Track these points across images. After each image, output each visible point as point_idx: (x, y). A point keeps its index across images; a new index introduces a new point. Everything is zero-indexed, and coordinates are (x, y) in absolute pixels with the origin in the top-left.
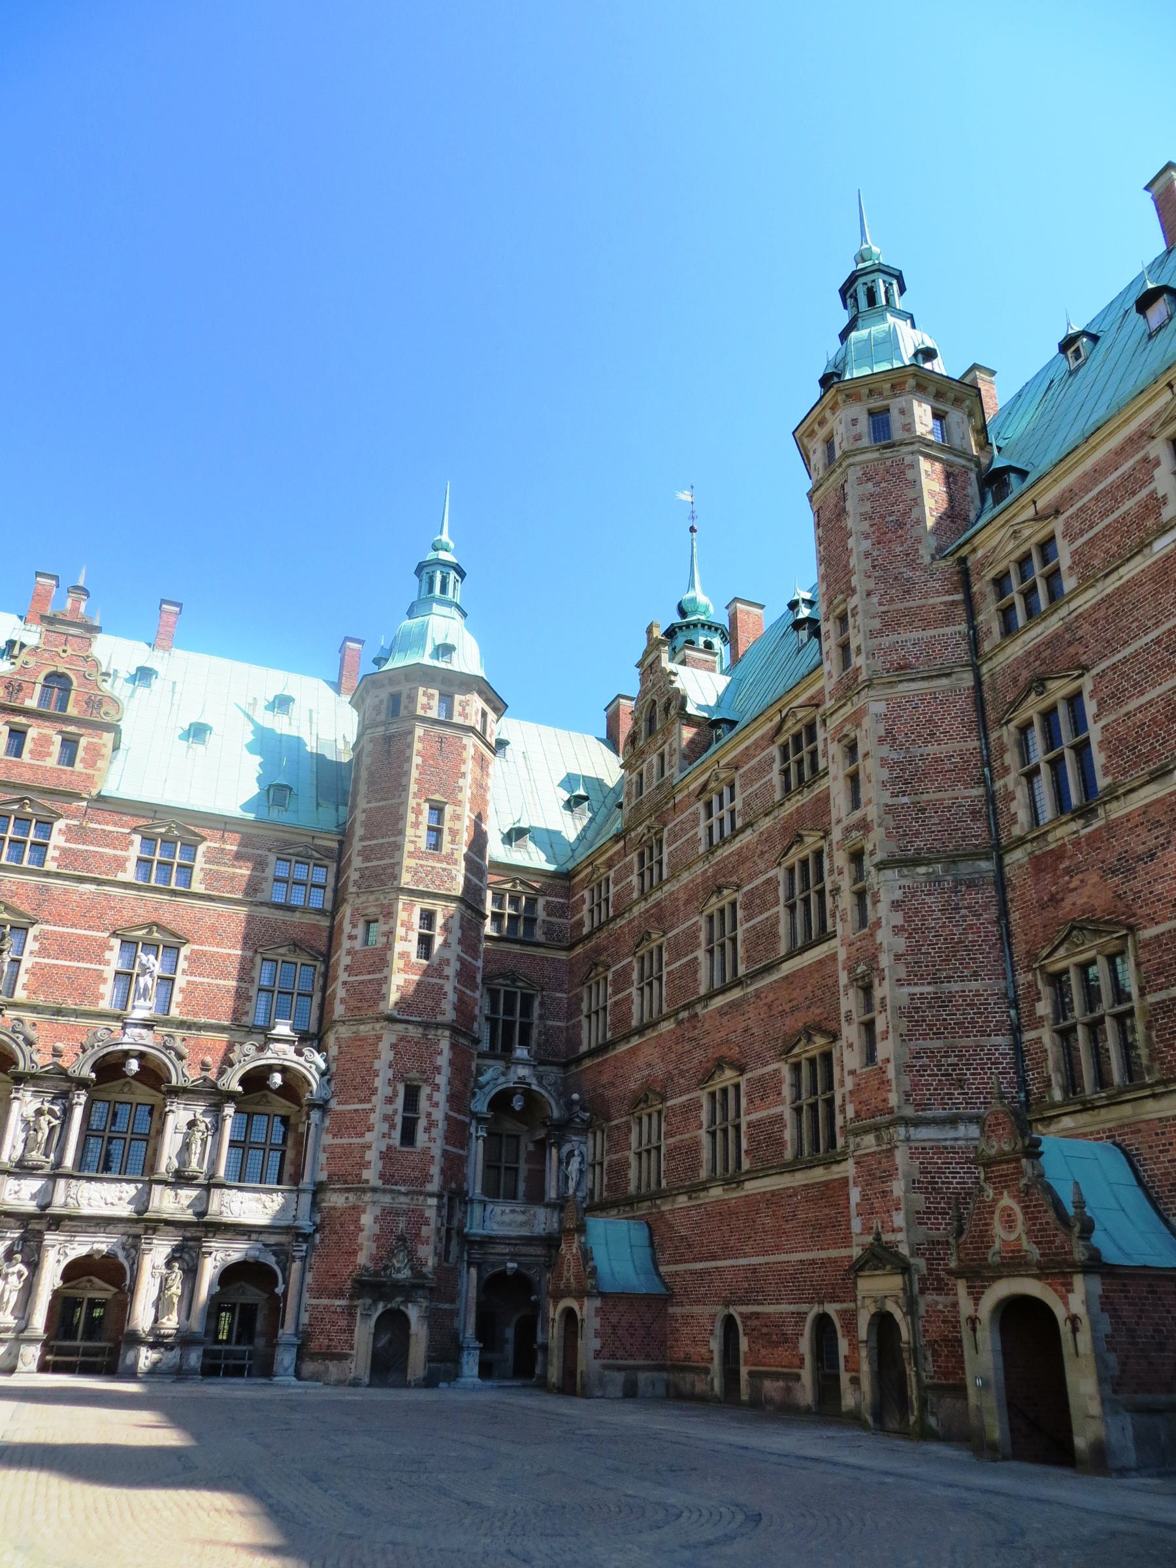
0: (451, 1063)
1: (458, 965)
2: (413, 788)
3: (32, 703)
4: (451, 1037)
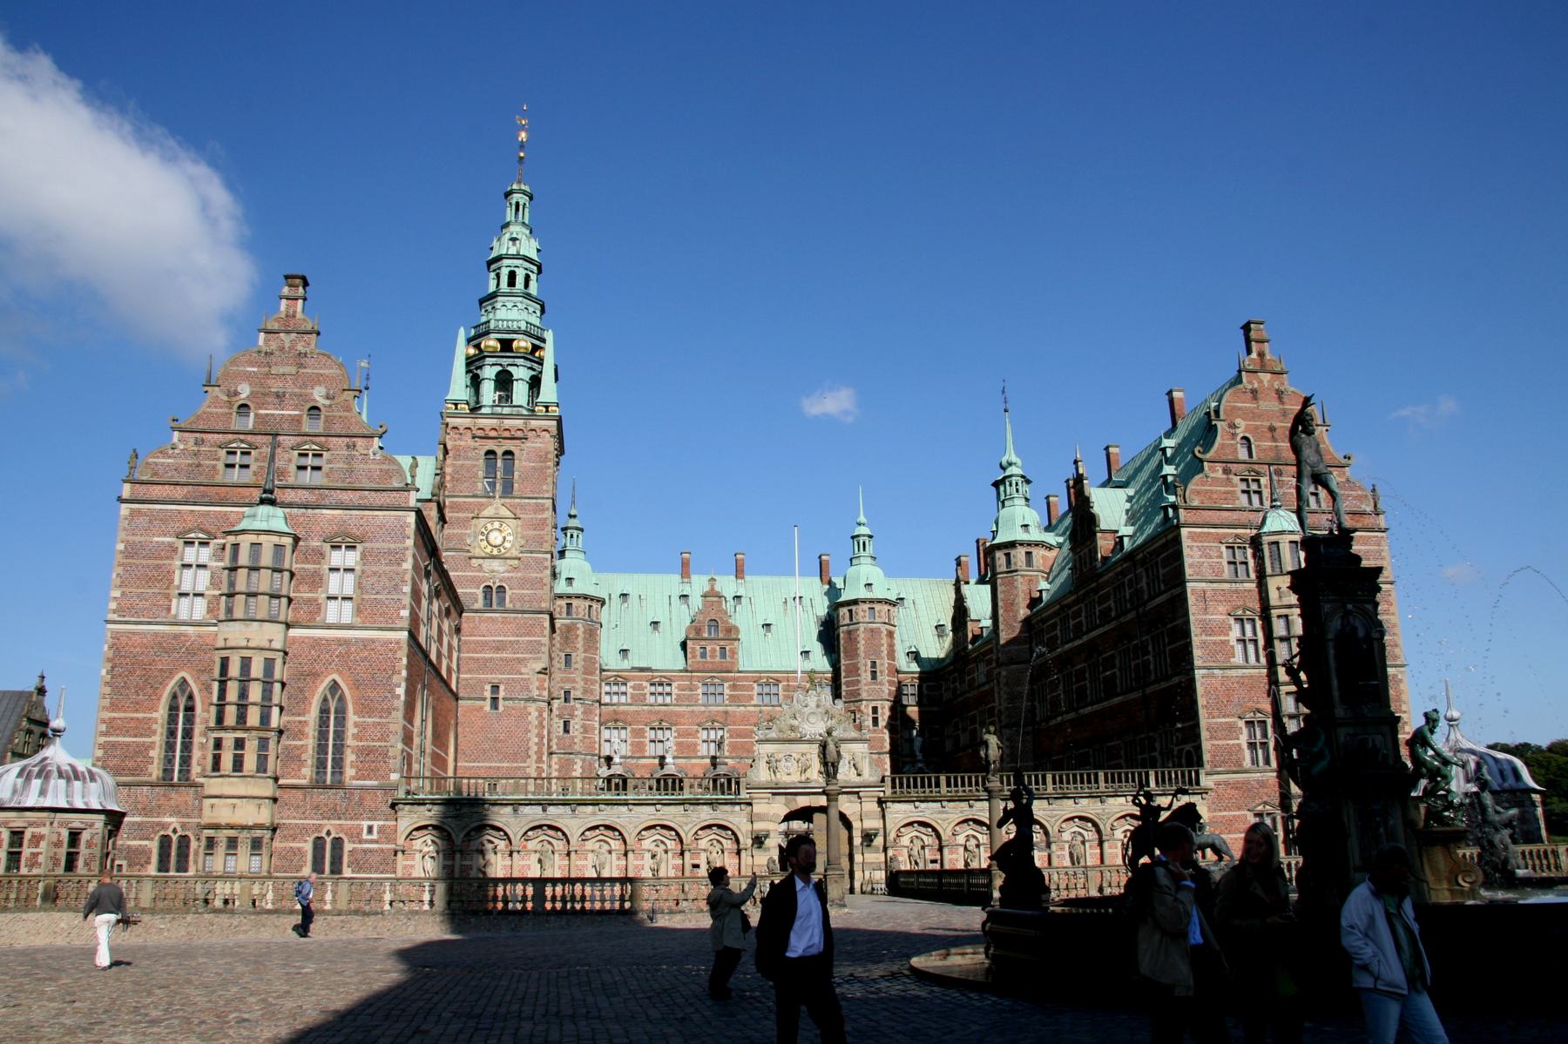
2: (862, 655)
3: (706, 635)
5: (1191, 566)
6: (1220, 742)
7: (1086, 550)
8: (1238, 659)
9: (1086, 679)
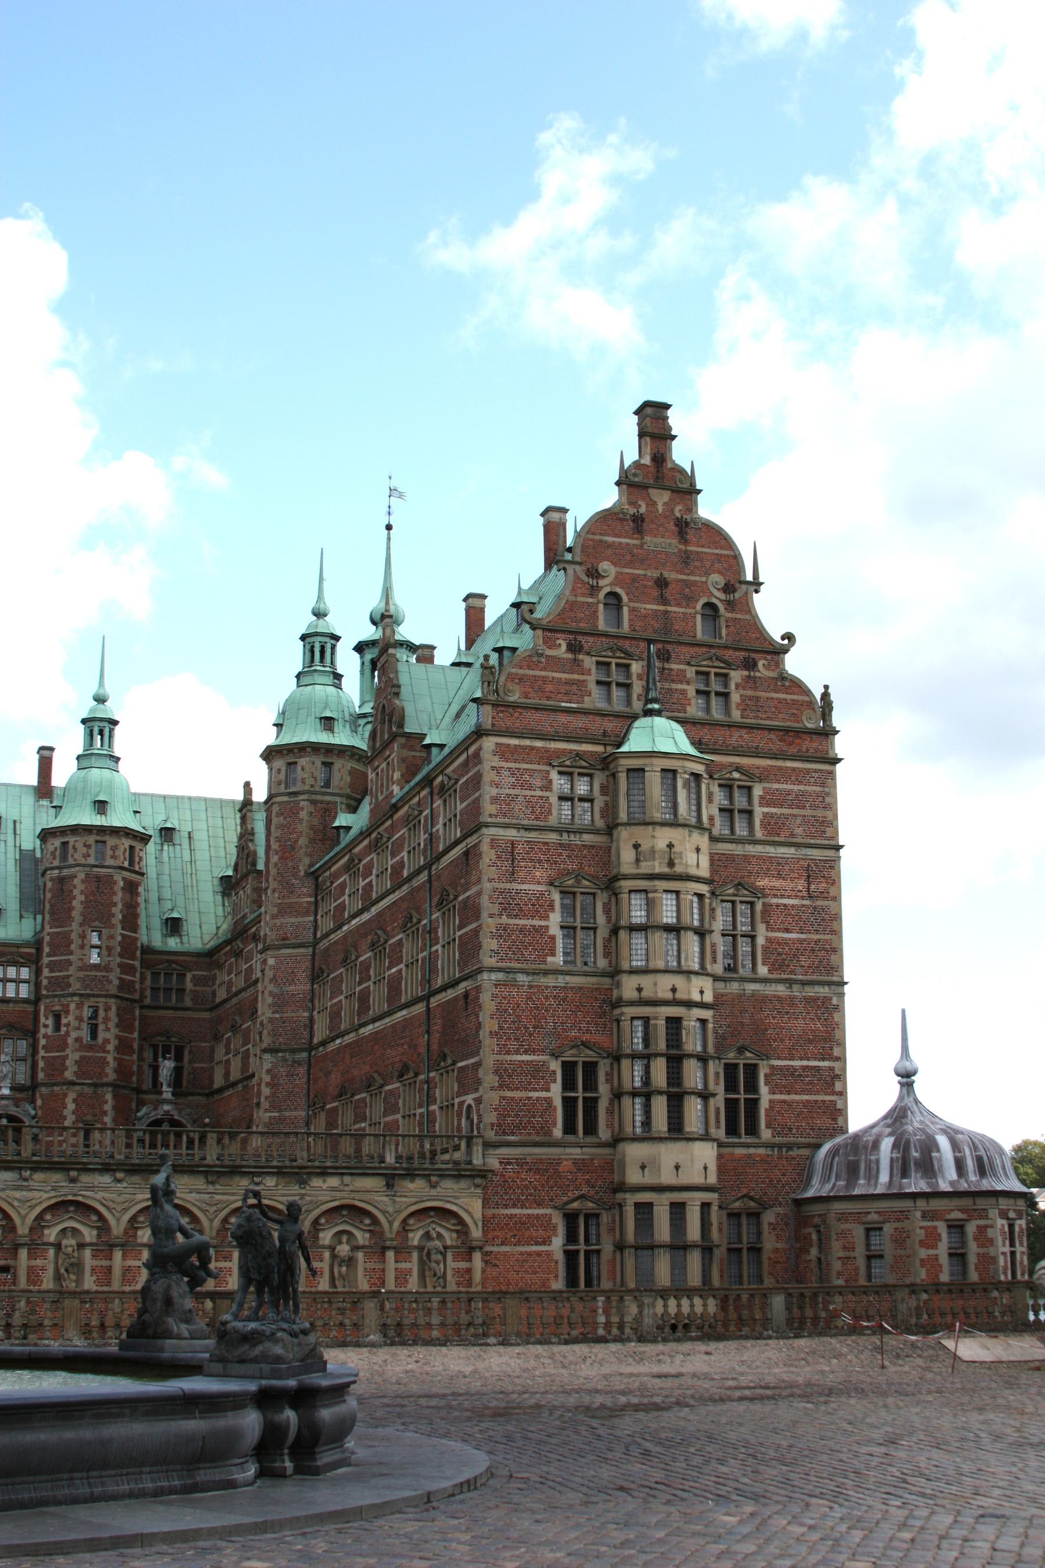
0: (114, 1107)
1: (117, 1042)
4: (113, 1091)
5: (494, 800)
6: (517, 1094)
7: (384, 765)
8: (558, 959)
9: (370, 979)
